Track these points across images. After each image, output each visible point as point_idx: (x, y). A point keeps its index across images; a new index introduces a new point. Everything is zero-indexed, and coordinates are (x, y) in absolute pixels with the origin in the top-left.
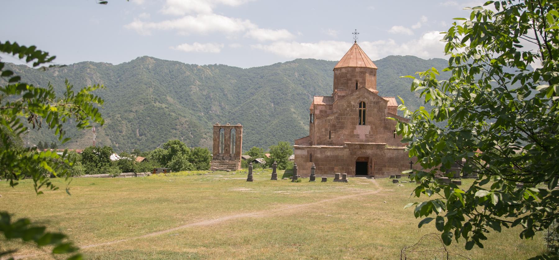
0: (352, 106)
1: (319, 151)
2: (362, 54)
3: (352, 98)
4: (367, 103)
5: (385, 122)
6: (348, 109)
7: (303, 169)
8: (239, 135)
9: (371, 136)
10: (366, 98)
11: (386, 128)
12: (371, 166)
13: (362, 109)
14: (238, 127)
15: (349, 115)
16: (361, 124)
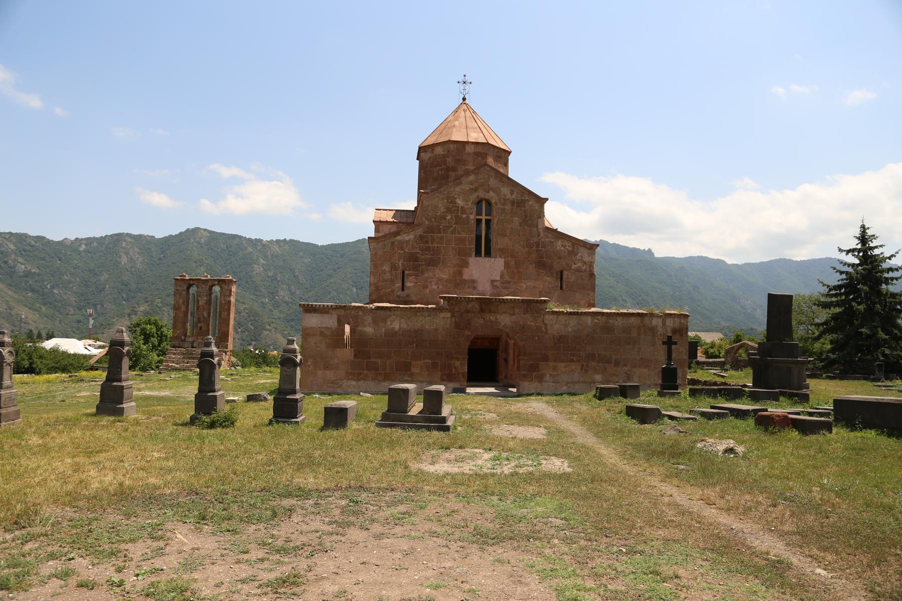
0: (458, 210)
1: (369, 319)
2: (478, 121)
3: (458, 189)
4: (496, 203)
5: (538, 251)
6: (449, 217)
7: (326, 368)
8: (227, 299)
9: (505, 284)
10: (492, 191)
11: (541, 264)
12: (506, 360)
13: (484, 218)
14: (224, 281)
15: (452, 233)
16: (481, 256)
